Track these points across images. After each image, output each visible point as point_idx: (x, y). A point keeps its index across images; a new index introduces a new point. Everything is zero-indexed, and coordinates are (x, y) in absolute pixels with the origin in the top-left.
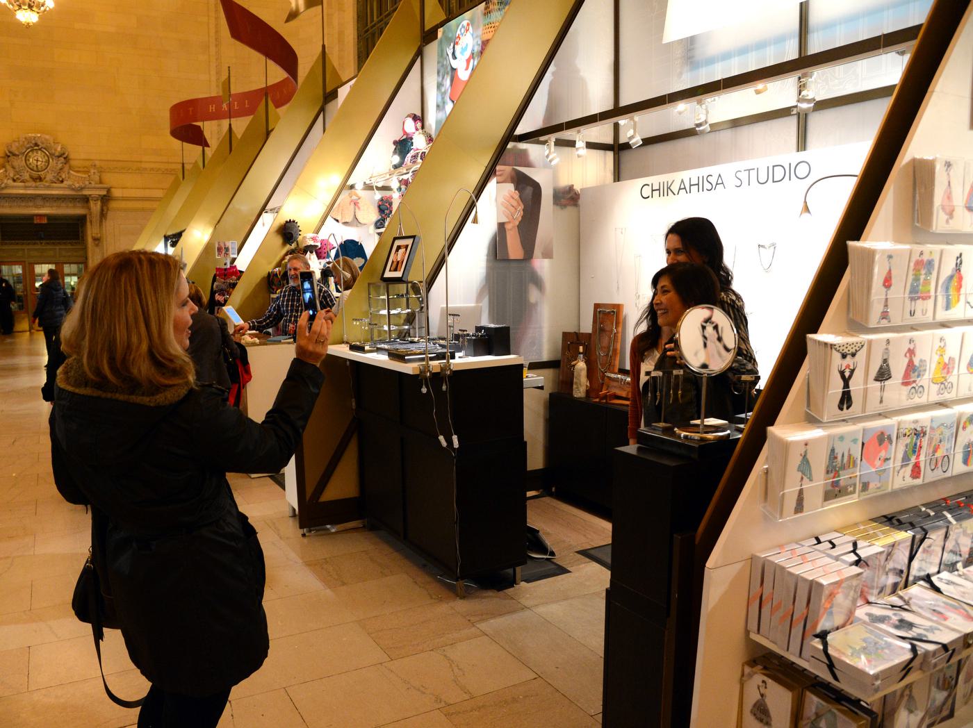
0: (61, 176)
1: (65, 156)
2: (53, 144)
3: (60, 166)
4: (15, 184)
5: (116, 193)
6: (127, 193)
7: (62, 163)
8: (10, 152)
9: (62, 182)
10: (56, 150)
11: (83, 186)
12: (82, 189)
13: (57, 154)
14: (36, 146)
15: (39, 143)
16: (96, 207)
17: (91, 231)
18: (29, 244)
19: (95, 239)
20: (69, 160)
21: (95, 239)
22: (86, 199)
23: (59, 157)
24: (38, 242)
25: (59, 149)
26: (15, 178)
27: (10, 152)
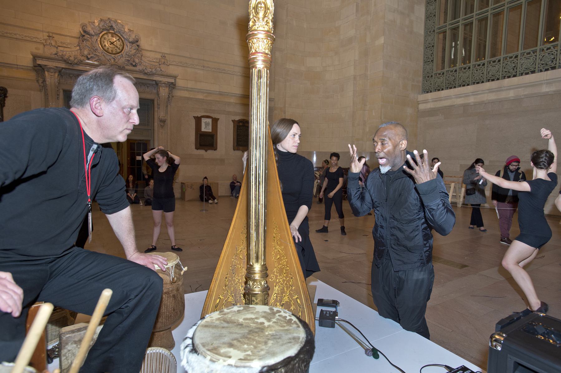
5: (180, 83)
6: (190, 85)
8: (85, 32)
12: (153, 74)
13: (131, 40)
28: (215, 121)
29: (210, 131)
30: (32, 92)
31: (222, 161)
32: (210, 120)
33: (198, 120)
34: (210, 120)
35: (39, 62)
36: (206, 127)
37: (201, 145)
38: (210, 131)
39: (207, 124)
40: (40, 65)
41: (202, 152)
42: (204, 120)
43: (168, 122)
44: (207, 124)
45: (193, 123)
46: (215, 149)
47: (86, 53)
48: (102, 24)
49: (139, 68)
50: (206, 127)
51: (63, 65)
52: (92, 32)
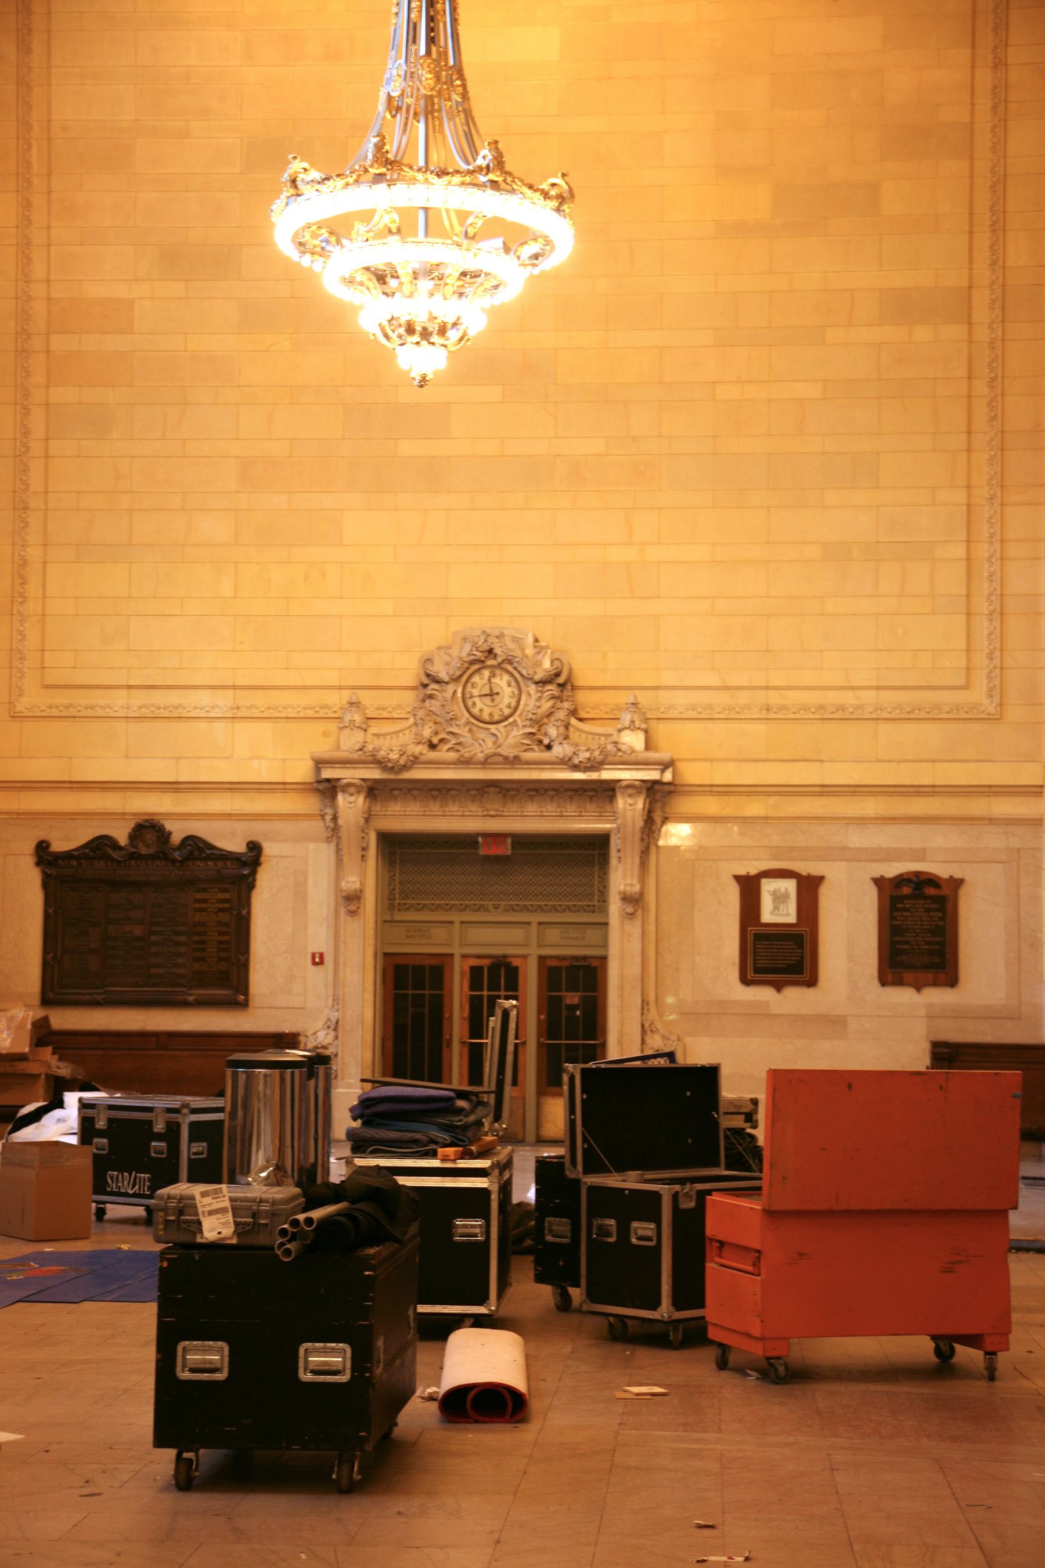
0: (546, 734)
1: (561, 680)
2: (530, 651)
3: (546, 705)
4: (433, 755)
6: (721, 775)
7: (553, 697)
8: (428, 675)
9: (549, 747)
10: (538, 664)
11: (599, 758)
14: (486, 658)
15: (498, 650)
16: (630, 808)
17: (621, 877)
18: (464, 909)
19: (626, 898)
20: (574, 688)
21: (626, 898)
22: (608, 791)
23: (543, 682)
24: (489, 903)
25: (547, 664)
26: (435, 740)
27: (428, 675)
28: (809, 888)
29: (792, 919)
30: (312, 846)
31: (834, 1024)
32: (789, 886)
33: (749, 888)
34: (789, 886)
35: (327, 774)
36: (776, 908)
37: (757, 970)
38: (792, 919)
39: (779, 898)
40: (328, 780)
41: (764, 994)
42: (768, 887)
43: (651, 898)
44: (779, 898)
45: (733, 894)
46: (812, 982)
47: (427, 732)
48: (467, 648)
49: (558, 751)
50: (778, 907)
51: (375, 774)
52: (443, 676)
